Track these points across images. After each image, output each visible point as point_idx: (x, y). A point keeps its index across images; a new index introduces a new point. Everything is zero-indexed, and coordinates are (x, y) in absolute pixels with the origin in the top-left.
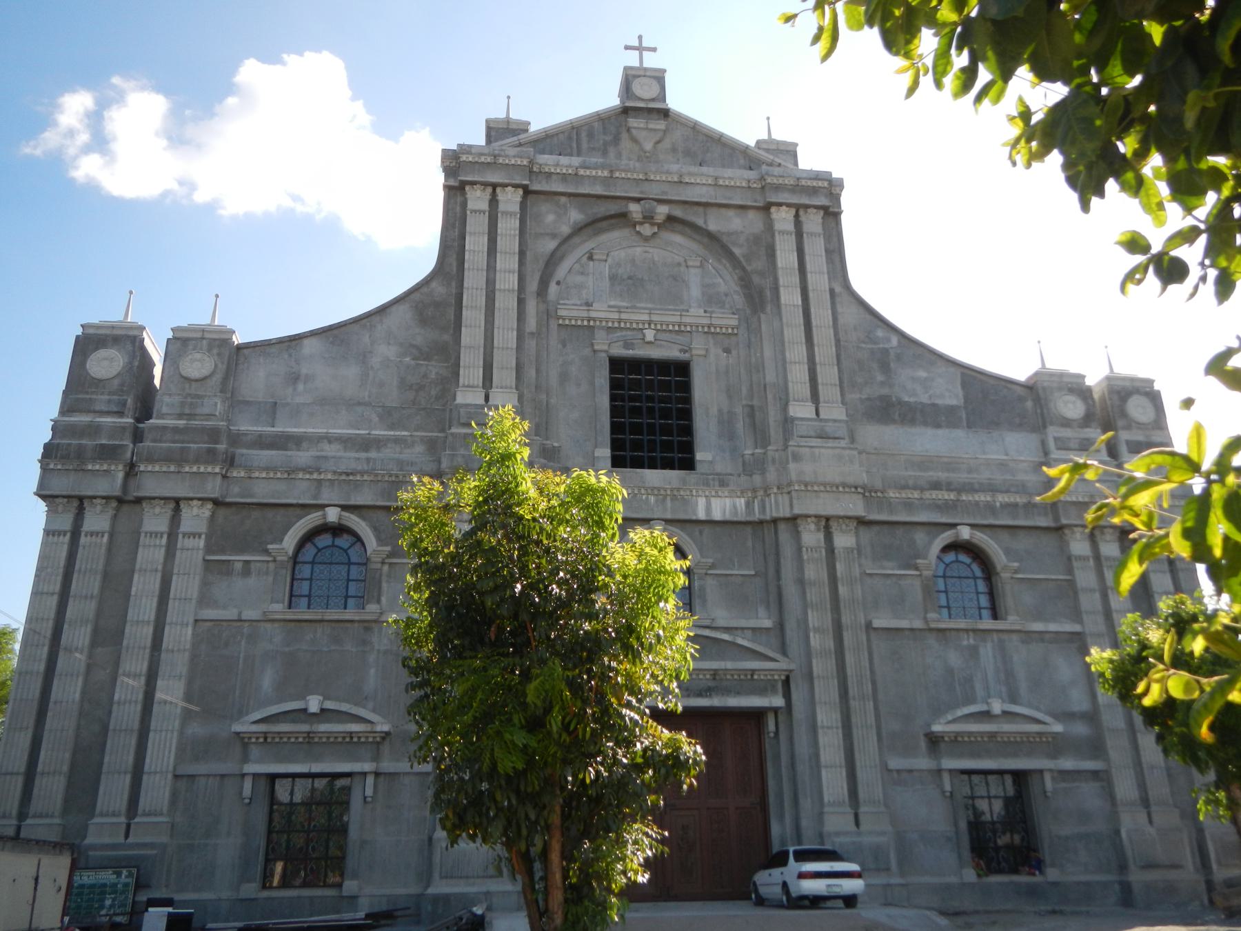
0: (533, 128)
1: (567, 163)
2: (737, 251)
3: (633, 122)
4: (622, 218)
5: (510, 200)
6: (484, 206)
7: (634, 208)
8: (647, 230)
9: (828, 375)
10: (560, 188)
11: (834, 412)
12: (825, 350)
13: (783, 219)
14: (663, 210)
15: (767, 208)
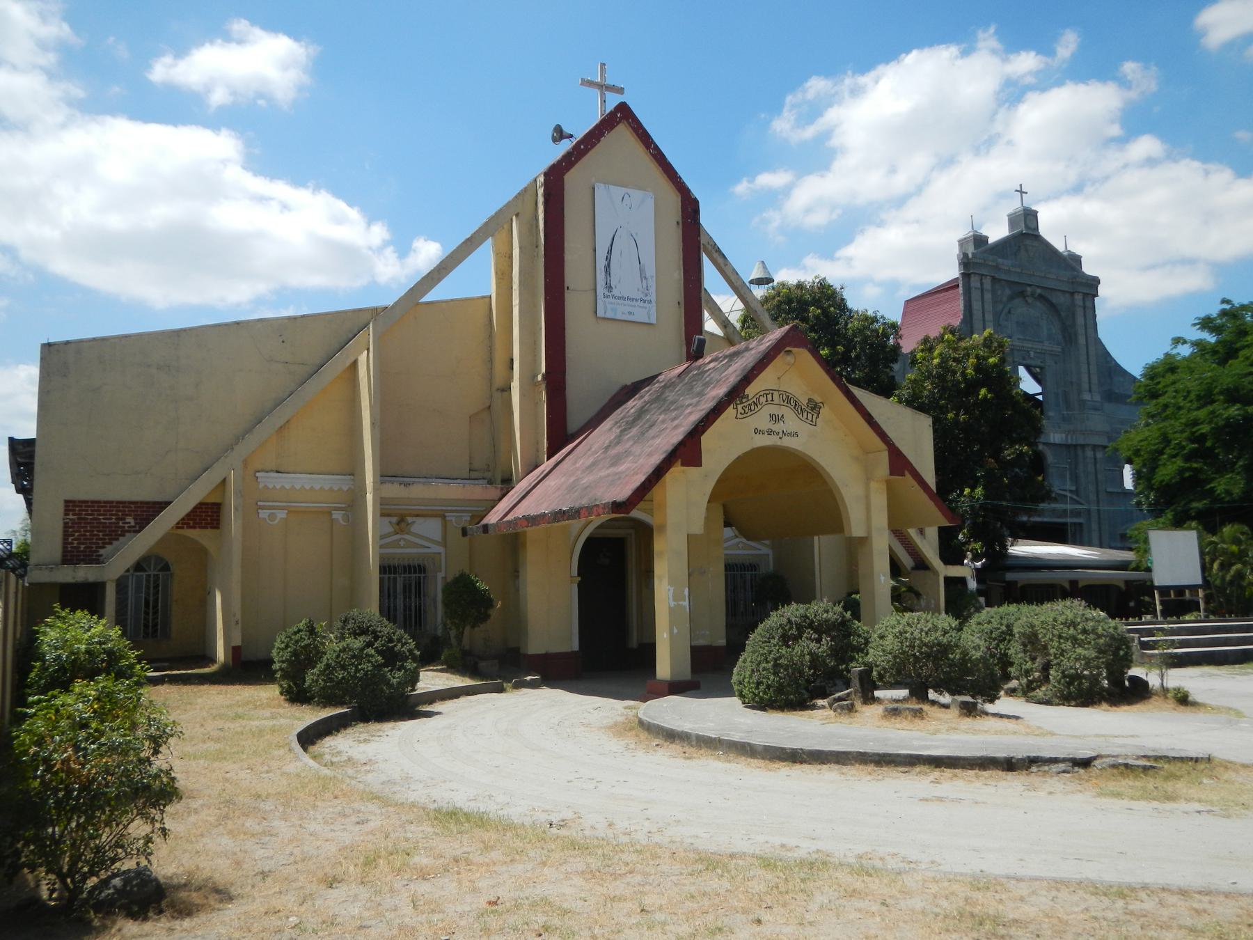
0: (990, 241)
1: (1006, 263)
2: (1063, 314)
3: (1028, 242)
4: (1022, 294)
5: (988, 283)
6: (978, 285)
7: (1029, 289)
8: (1030, 300)
9: (1095, 379)
10: (1004, 277)
11: (1097, 398)
12: (1093, 369)
13: (1078, 297)
14: (1039, 291)
15: (1072, 294)
